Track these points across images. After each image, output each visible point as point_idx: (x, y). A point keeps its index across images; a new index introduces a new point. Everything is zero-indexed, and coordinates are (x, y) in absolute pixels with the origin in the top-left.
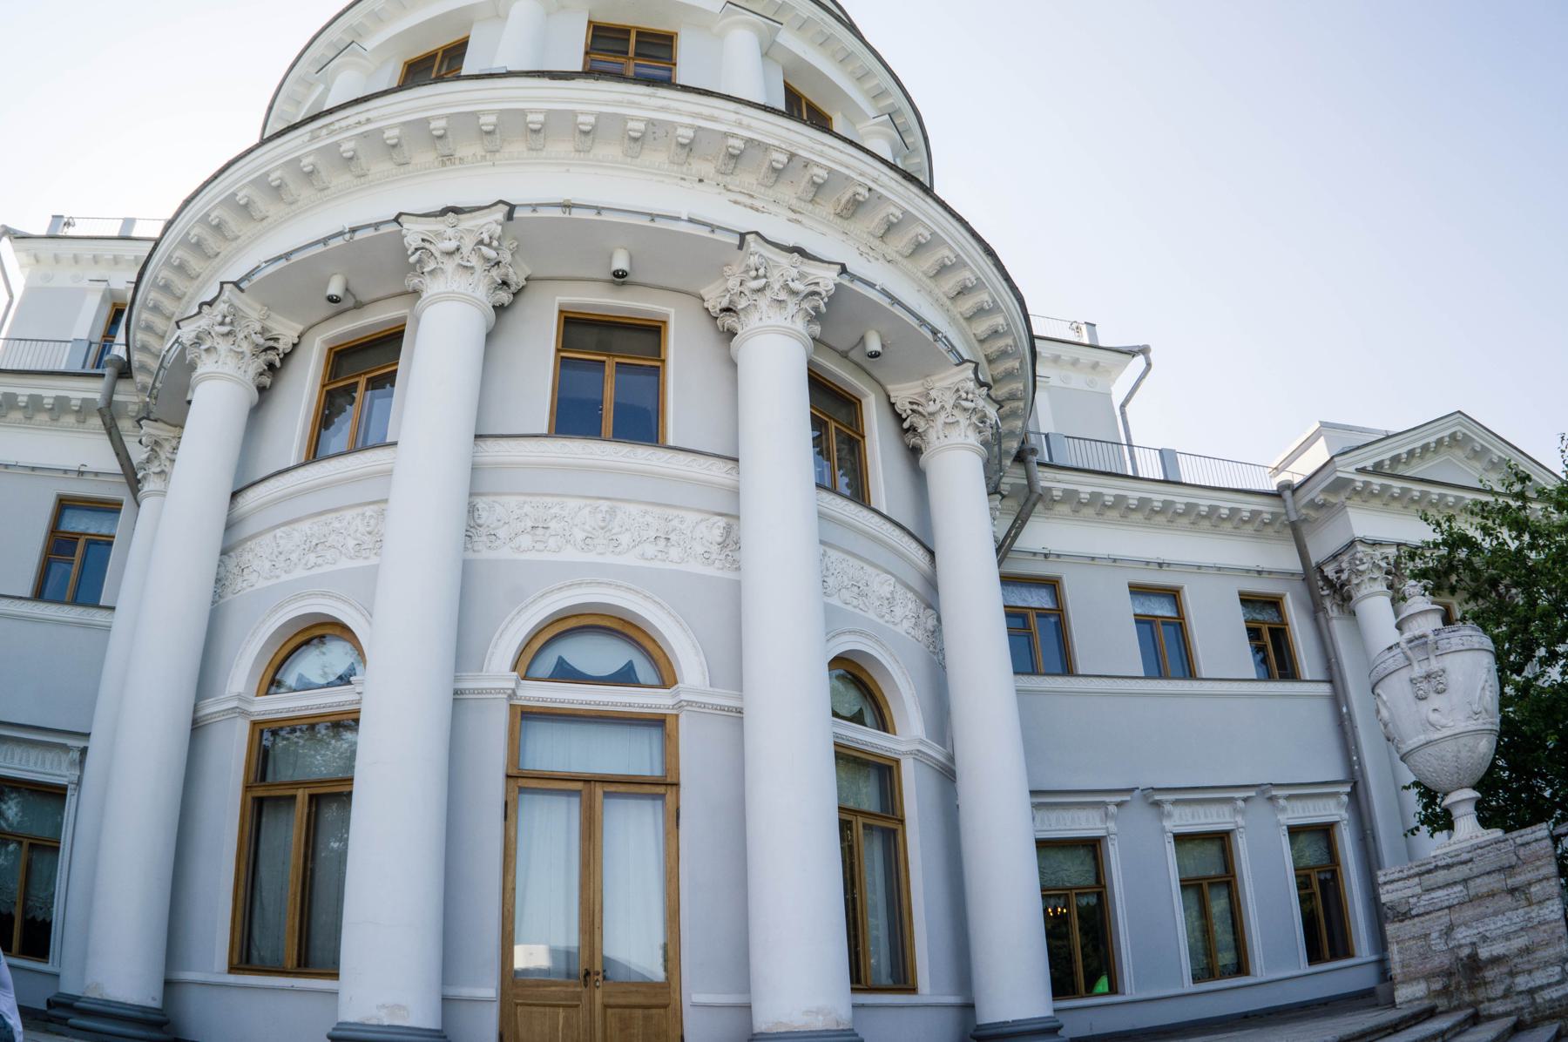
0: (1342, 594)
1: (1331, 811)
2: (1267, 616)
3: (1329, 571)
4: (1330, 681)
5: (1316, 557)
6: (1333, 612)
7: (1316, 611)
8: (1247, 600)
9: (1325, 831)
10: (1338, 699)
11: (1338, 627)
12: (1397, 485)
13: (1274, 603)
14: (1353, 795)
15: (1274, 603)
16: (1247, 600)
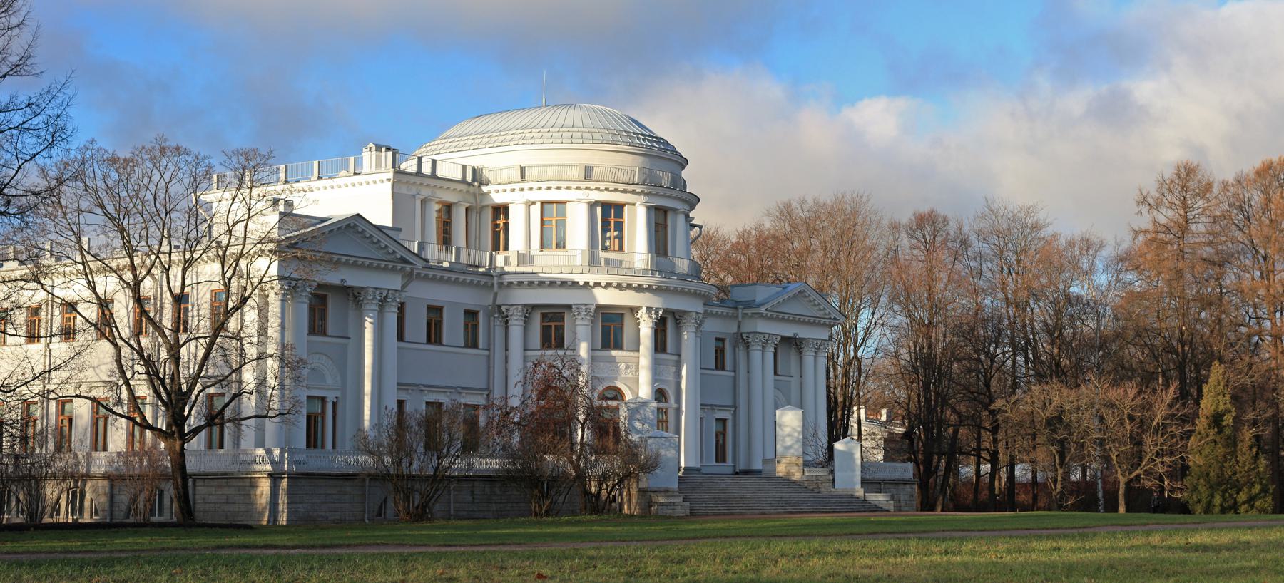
0: (747, 345)
1: (726, 415)
2: (720, 344)
3: (744, 336)
4: (734, 371)
5: (742, 331)
6: (741, 348)
7: (735, 347)
8: (717, 339)
9: (724, 421)
10: (735, 379)
11: (741, 354)
12: (775, 315)
13: (723, 340)
14: (735, 411)
15: (723, 340)
16: (717, 339)
